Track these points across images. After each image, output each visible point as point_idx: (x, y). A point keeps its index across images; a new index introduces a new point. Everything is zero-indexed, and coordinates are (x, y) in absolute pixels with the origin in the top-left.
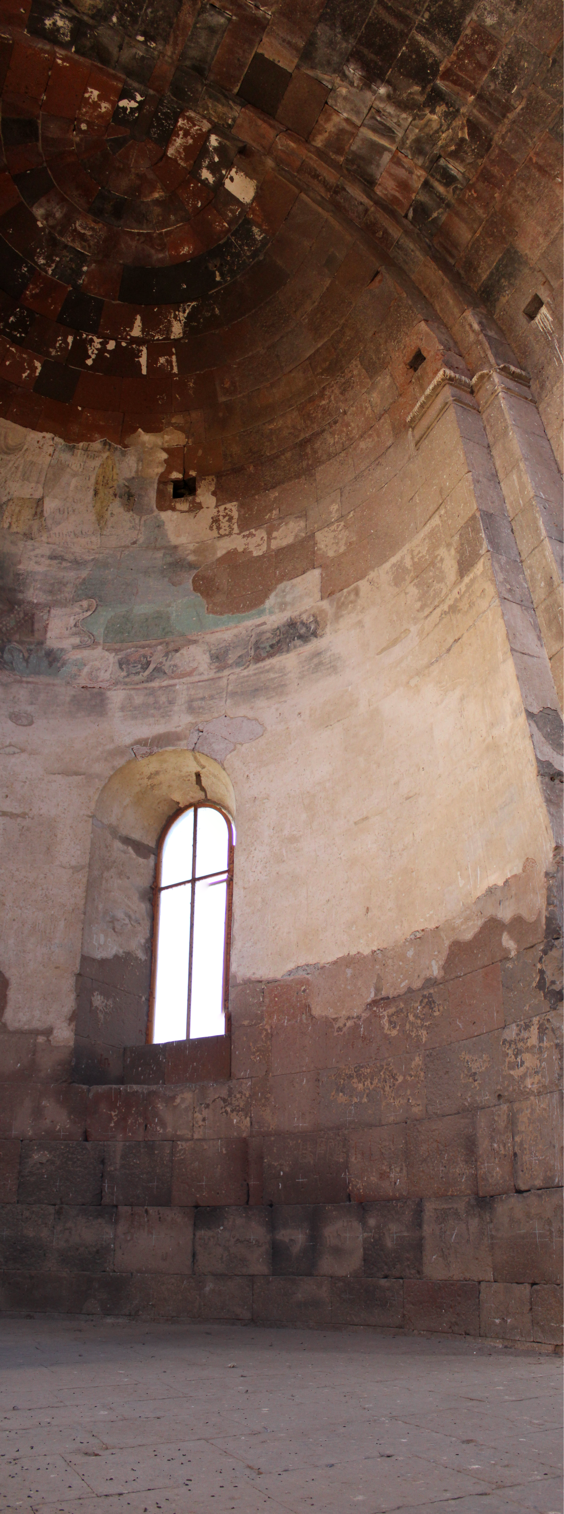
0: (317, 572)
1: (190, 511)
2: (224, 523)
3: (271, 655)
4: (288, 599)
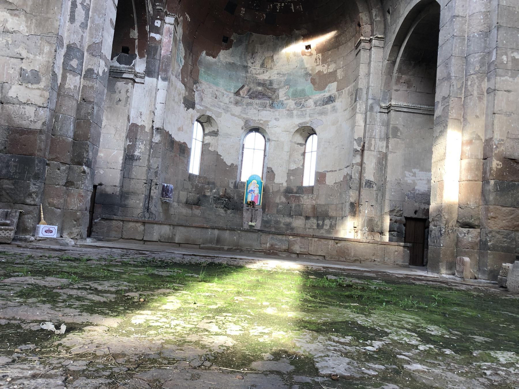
0: (337, 82)
1: (310, 55)
2: (318, 61)
3: (326, 104)
4: (330, 89)
